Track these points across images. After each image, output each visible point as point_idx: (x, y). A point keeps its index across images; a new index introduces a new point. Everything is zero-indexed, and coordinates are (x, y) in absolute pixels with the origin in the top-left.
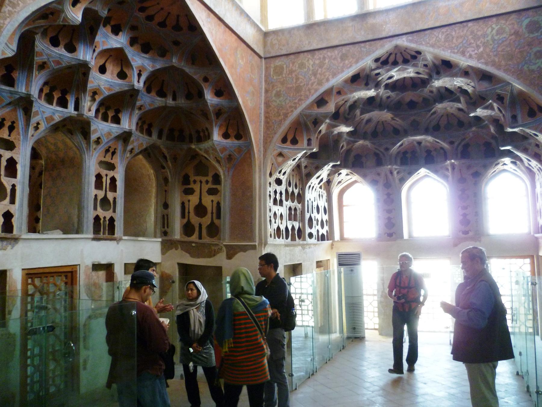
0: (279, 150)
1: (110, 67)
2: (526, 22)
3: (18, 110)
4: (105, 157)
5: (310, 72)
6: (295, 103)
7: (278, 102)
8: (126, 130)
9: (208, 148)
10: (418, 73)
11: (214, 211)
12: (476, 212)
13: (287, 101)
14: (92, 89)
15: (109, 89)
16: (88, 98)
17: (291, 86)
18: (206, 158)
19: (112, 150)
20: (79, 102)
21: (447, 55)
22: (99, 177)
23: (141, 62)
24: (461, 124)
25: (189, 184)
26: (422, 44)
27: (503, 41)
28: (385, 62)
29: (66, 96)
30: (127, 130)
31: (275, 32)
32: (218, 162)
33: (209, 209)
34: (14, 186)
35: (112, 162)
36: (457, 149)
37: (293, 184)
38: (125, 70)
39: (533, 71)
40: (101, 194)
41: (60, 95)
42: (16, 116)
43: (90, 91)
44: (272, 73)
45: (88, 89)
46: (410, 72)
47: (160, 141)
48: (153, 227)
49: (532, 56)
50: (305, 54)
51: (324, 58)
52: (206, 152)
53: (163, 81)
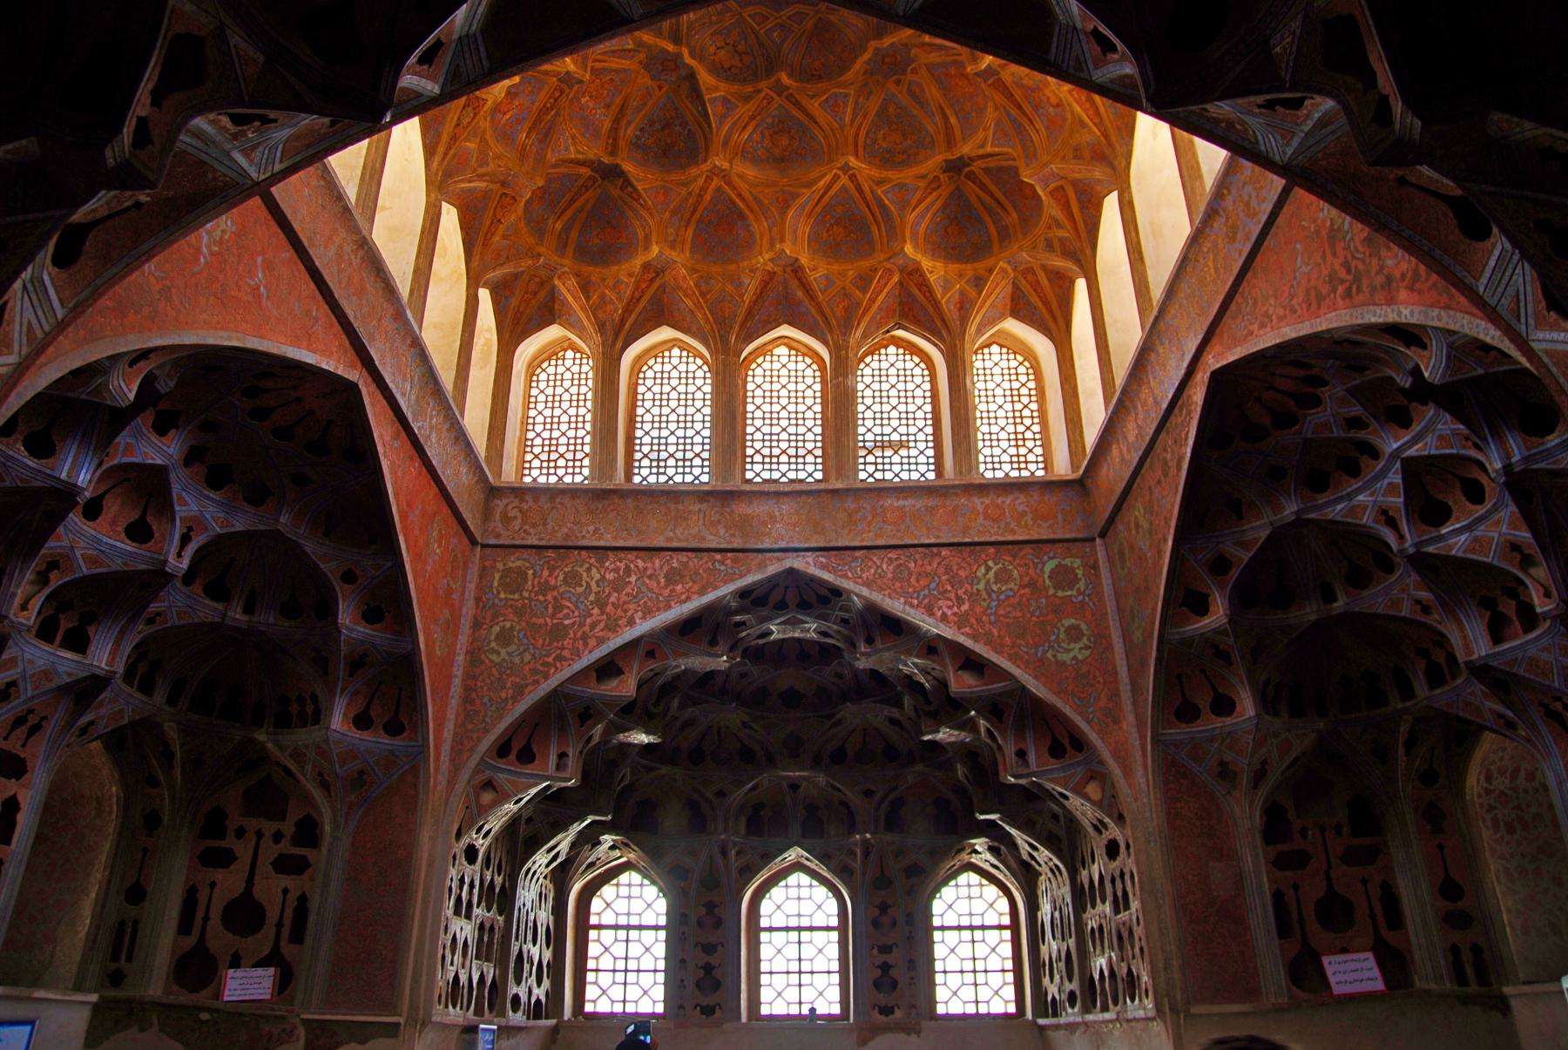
0: (488, 774)
1: (112, 507)
2: (1050, 565)
5: (592, 598)
6: (546, 664)
7: (503, 652)
8: (98, 672)
9: (307, 747)
10: (824, 634)
11: (287, 921)
12: (911, 961)
13: (527, 657)
16: (29, 575)
17: (541, 621)
18: (287, 771)
21: (896, 606)
24: (891, 754)
25: (223, 837)
26: (845, 576)
27: (1008, 598)
28: (756, 599)
31: (519, 492)
32: (325, 786)
33: (273, 914)
36: (877, 810)
37: (494, 862)
38: (150, 519)
39: (1064, 663)
44: (496, 584)
46: (810, 629)
48: (77, 957)
49: (1062, 636)
50: (584, 553)
51: (628, 571)
52: (298, 756)
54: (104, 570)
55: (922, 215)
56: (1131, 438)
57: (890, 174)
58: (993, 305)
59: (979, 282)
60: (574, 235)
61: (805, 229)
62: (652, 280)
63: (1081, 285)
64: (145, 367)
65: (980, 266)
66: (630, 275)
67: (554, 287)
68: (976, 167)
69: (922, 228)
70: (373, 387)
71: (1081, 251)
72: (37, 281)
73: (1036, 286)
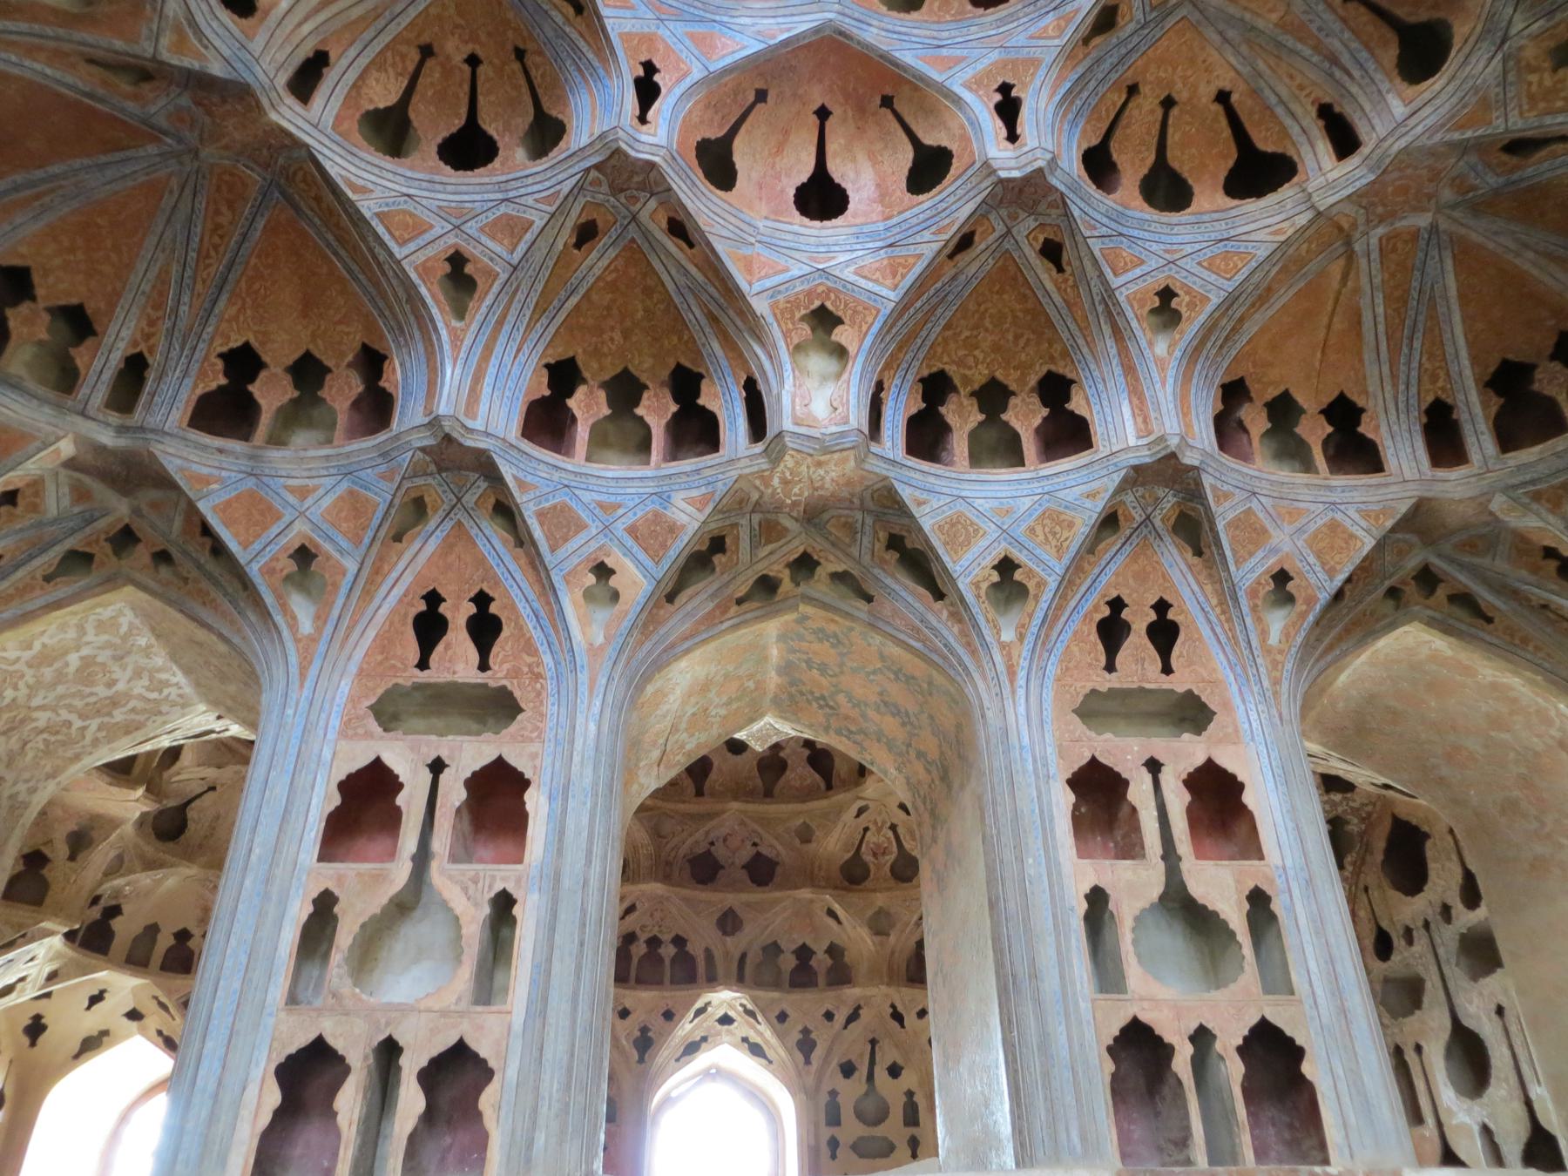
3: (474, 531)
4: (1110, 667)
14: (794, 304)
15: (894, 269)
19: (1139, 618)
20: (759, 395)
22: (1098, 791)
29: (701, 402)
30: (1145, 457)
34: (504, 904)
35: (1179, 683)
38: (929, 140)
40: (1135, 884)
41: (674, 408)
42: (481, 562)
43: (784, 313)
45: (761, 306)
47: (1455, 474)
53: (1223, 97)
54: (918, 269)
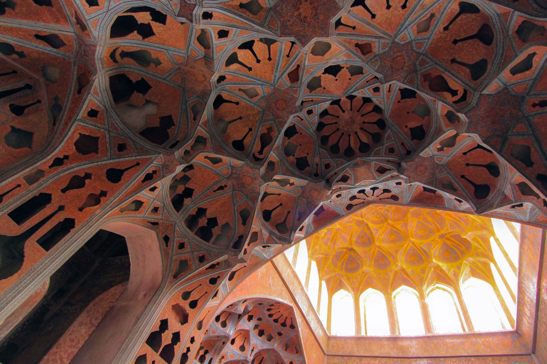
23: (257, 343)
31: (335, 338)
55: (436, 251)
56: (528, 313)
57: (424, 241)
58: (465, 274)
59: (459, 268)
60: (344, 266)
61: (403, 258)
62: (365, 276)
63: (492, 265)
64: (246, 303)
65: (458, 263)
66: (359, 275)
67: (341, 280)
68: (448, 236)
69: (437, 254)
70: (297, 308)
71: (488, 255)
72: (225, 284)
73: (478, 267)
